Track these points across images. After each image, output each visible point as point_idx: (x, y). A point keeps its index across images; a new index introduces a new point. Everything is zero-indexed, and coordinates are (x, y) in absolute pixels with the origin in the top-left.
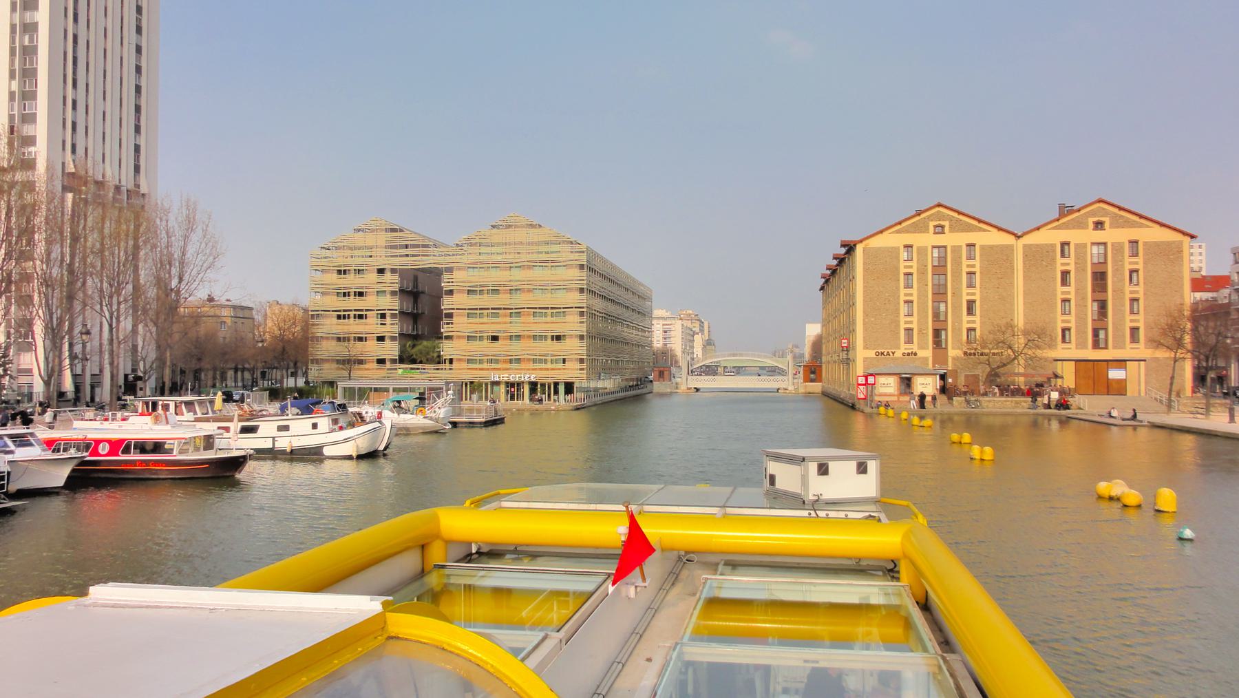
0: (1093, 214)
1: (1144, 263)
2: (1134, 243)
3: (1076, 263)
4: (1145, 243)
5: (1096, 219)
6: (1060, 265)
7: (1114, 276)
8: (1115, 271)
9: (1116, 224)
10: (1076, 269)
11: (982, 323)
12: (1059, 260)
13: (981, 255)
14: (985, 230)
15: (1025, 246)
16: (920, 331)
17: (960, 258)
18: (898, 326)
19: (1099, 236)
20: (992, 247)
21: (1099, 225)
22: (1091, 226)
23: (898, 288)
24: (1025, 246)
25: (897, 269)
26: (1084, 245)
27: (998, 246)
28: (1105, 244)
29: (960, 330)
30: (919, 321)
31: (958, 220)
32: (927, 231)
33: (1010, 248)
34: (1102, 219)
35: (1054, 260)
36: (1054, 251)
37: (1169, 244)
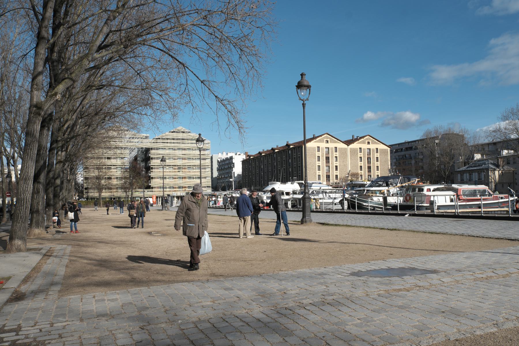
0: (367, 139)
1: (380, 155)
2: (336, 148)
3: (363, 154)
4: (380, 149)
5: (368, 141)
6: (360, 155)
7: (372, 159)
8: (373, 157)
9: (373, 143)
10: (363, 156)
11: (340, 173)
12: (359, 154)
13: (339, 151)
14: (339, 143)
15: (350, 148)
16: (322, 176)
17: (333, 151)
18: (316, 174)
19: (327, 145)
20: (341, 148)
21: (369, 143)
22: (367, 143)
23: (316, 161)
24: (350, 148)
25: (315, 154)
26: (365, 149)
27: (343, 148)
28: (328, 148)
29: (334, 175)
30: (322, 172)
31: (332, 139)
32: (323, 142)
33: (346, 149)
34: (369, 141)
35: (358, 153)
36: (358, 151)
37: (385, 150)
